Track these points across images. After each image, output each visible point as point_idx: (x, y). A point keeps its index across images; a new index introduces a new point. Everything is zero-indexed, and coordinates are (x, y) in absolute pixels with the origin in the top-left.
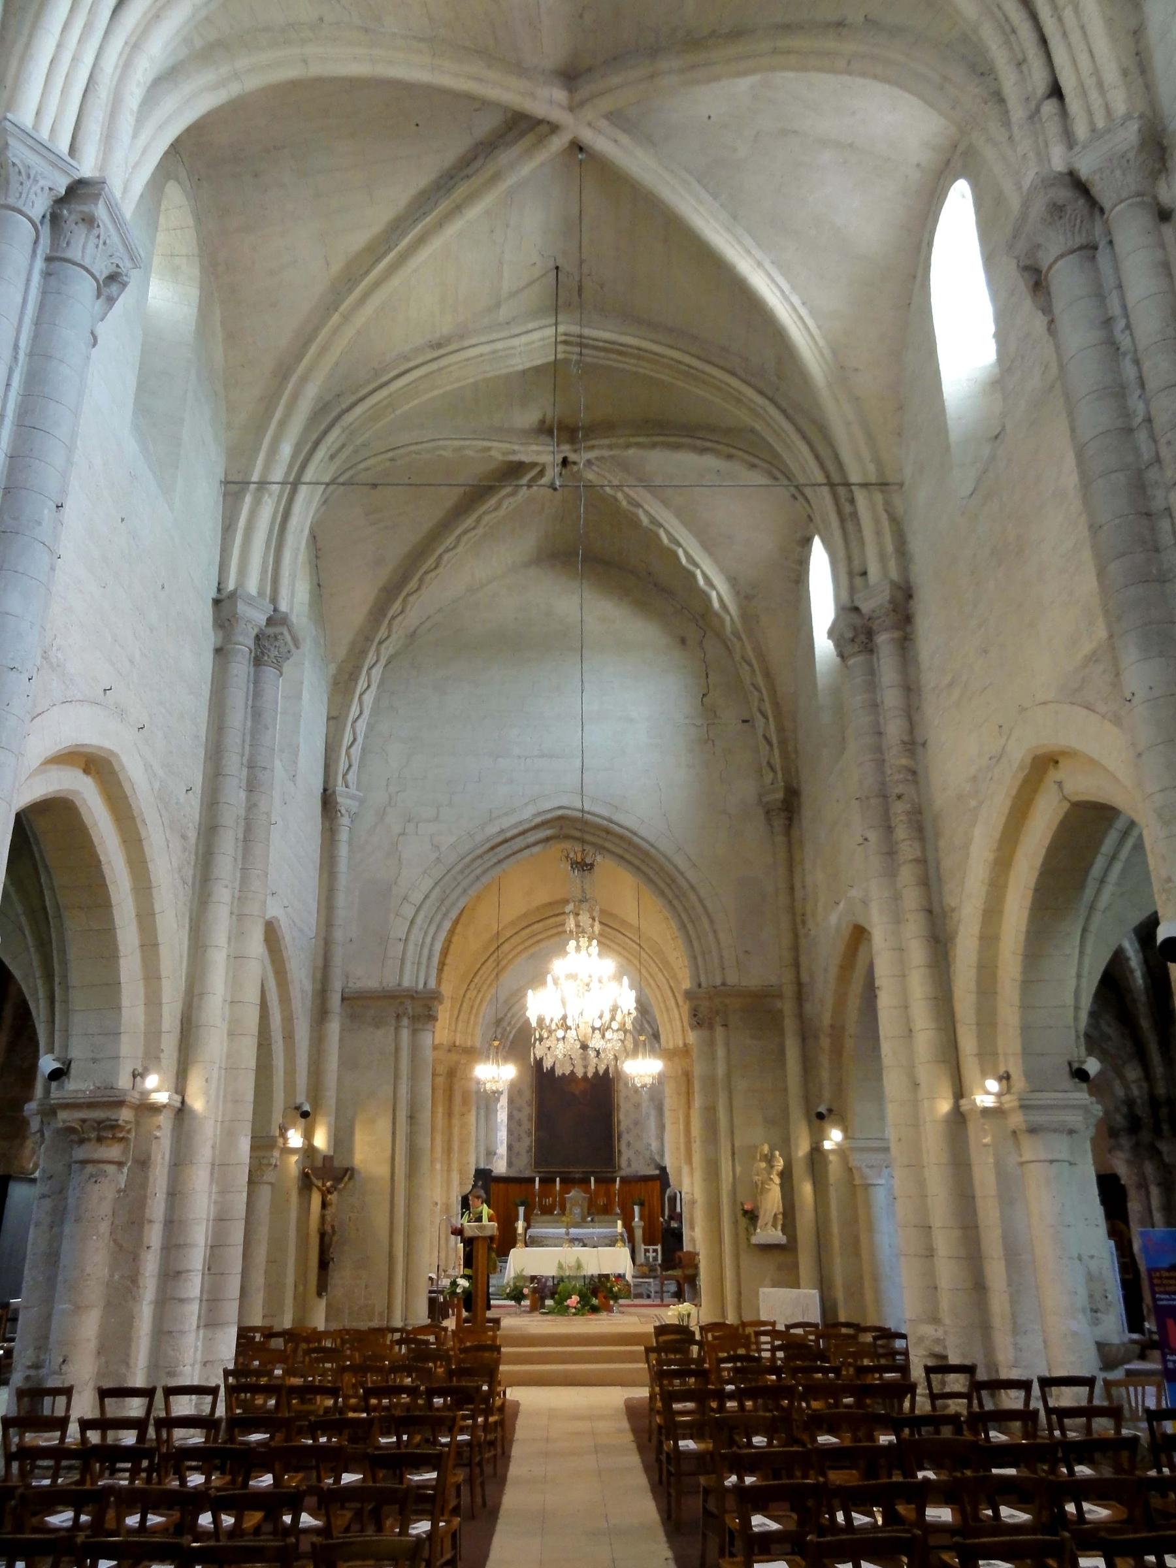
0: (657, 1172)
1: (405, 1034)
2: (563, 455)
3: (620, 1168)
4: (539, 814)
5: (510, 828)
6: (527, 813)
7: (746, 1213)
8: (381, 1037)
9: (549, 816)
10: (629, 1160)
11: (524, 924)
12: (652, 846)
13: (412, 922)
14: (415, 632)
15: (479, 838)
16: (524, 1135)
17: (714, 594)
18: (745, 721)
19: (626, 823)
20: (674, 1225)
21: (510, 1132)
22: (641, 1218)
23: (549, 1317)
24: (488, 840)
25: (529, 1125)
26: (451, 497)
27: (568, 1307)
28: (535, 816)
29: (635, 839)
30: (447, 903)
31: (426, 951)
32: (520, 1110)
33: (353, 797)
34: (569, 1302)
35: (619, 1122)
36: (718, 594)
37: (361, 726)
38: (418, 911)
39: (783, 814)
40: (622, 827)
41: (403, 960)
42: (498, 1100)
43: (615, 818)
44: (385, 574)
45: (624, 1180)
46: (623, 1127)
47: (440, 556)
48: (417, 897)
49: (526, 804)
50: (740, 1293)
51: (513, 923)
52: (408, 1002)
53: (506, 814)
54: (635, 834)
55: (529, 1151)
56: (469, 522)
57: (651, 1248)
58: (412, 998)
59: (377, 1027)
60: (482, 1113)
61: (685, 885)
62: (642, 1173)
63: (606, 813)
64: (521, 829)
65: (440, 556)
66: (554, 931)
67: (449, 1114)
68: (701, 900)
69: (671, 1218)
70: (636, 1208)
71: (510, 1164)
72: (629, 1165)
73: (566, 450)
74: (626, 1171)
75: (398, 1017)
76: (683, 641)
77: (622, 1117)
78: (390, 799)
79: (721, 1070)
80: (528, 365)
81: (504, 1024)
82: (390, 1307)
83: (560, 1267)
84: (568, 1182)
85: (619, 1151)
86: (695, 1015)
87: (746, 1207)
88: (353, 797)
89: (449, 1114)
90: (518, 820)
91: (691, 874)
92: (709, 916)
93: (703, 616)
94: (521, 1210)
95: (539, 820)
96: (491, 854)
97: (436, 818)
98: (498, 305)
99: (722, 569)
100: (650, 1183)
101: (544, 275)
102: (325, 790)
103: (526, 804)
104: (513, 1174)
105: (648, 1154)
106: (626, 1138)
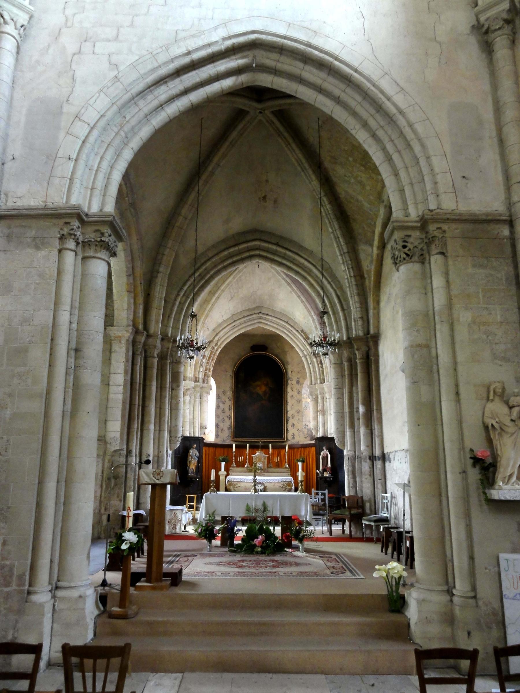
0: (313, 442)
1: (69, 258)
3: (287, 440)
4: (230, 38)
5: (197, 50)
6: (216, 37)
7: (476, 461)
8: (45, 259)
9: (241, 40)
10: (293, 435)
11: (223, 247)
12: (356, 71)
13: (84, 142)
15: (163, 58)
16: (227, 419)
19: (327, 47)
20: (326, 475)
21: (217, 416)
22: (303, 470)
23: (237, 558)
24: (172, 60)
25: (230, 413)
27: (255, 546)
28: (224, 39)
29: (336, 63)
30: (126, 129)
31: (101, 177)
32: (224, 403)
34: (256, 541)
35: (287, 412)
38: (92, 128)
39: (507, 29)
41: (71, 180)
42: (208, 393)
43: (315, 42)
45: (290, 447)
46: (290, 415)
48: (91, 116)
49: (216, 28)
50: (472, 558)
51: (214, 246)
52: (76, 223)
53: (193, 36)
54: (336, 59)
55: (229, 428)
57: (320, 492)
58: (82, 222)
59: (37, 248)
60: (198, 400)
61: (393, 110)
62: (301, 443)
63: (303, 37)
64: (210, 50)
66: (247, 254)
67: (161, 388)
68: (411, 126)
69: (324, 470)
70: (300, 464)
71: (217, 436)
72: (293, 438)
74: (291, 441)
75: (62, 238)
77: (289, 408)
78: (67, 20)
79: (439, 300)
81: (213, 344)
82: (33, 568)
83: (248, 510)
84: (254, 447)
85: (287, 429)
86: (404, 247)
87: (479, 455)
89: (161, 388)
90: (206, 42)
91: (399, 99)
92: (419, 139)
94: (223, 464)
95: (229, 43)
96: (177, 80)
97: (116, 38)
100: (307, 450)
103: (216, 28)
104: (219, 442)
105: (306, 431)
106: (291, 422)
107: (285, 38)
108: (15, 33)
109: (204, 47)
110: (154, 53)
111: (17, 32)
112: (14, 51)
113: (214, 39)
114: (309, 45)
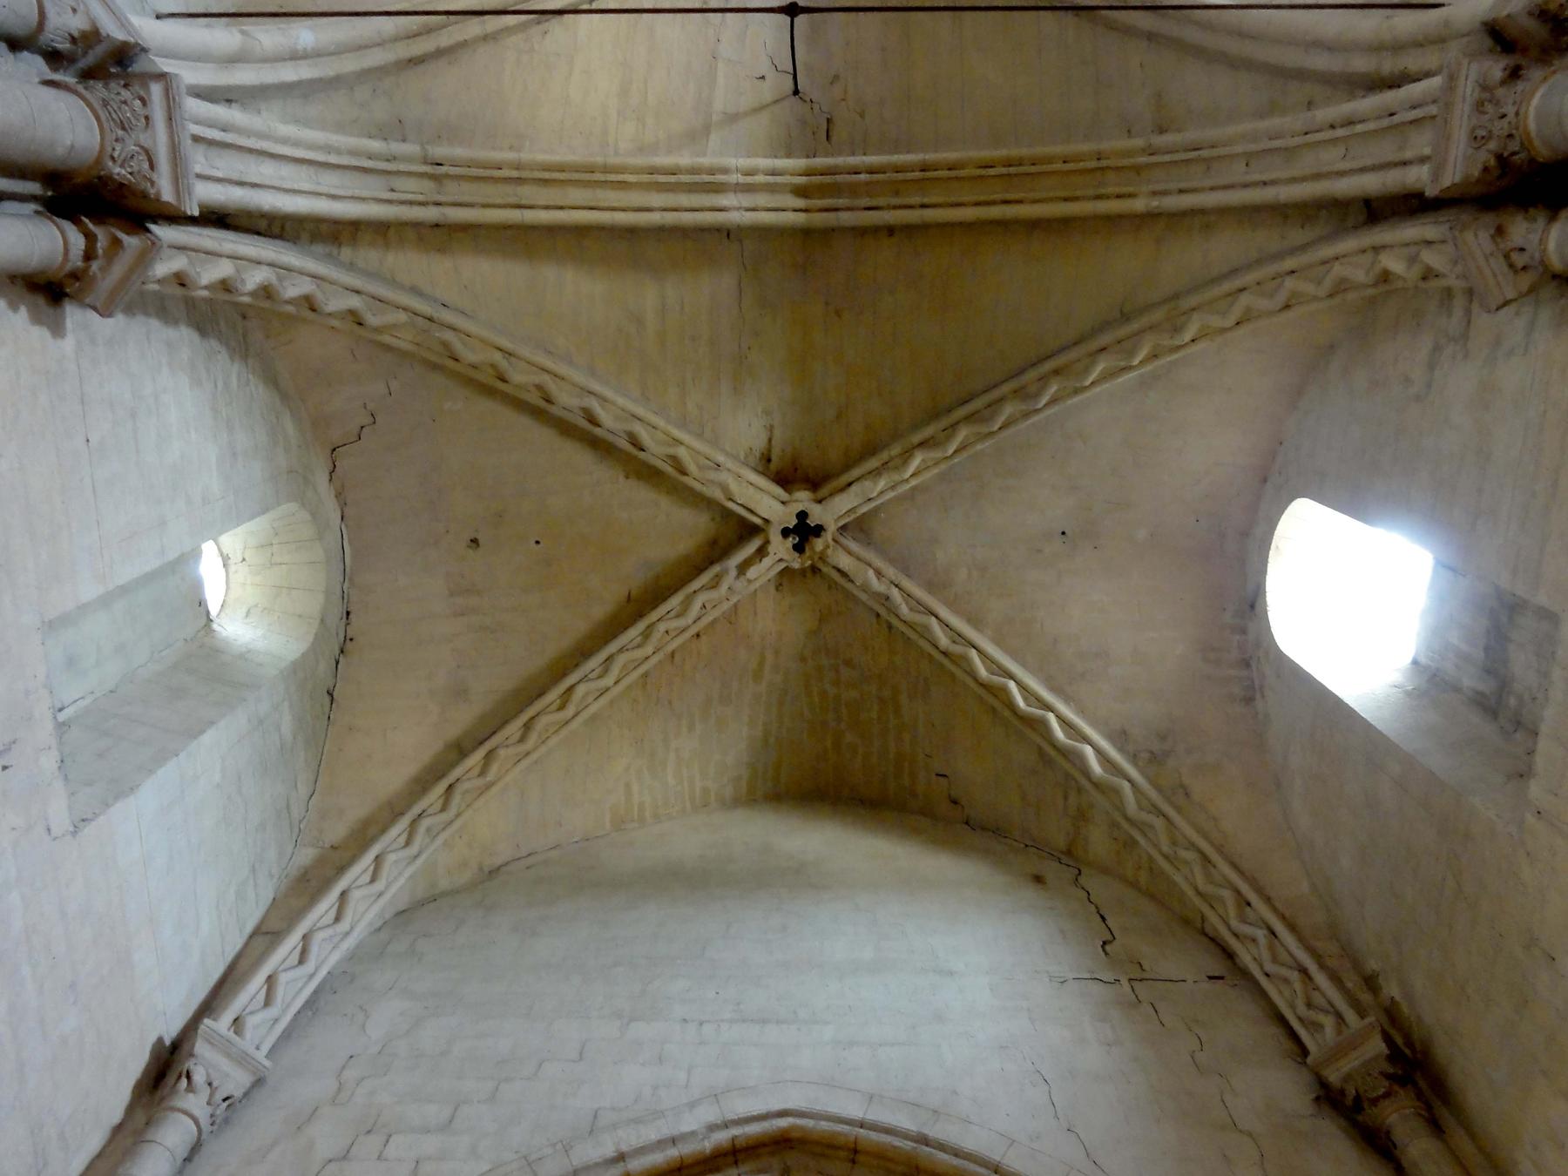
2: (800, 507)
4: (726, 1125)
6: (691, 1122)
9: (754, 1129)
14: (498, 868)
17: (1088, 751)
18: (1210, 978)
19: (969, 1143)
26: (605, 599)
28: (712, 1128)
33: (243, 1059)
36: (1098, 751)
37: (328, 955)
40: (957, 1153)
43: (936, 1131)
44: (462, 718)
47: (571, 689)
49: (692, 1105)
53: (637, 1121)
56: (634, 633)
65: (571, 689)
73: (803, 499)
76: (1038, 879)
78: (339, 1090)
80: (748, 218)
88: (243, 1059)
93: (1069, 853)
95: (722, 1137)
97: (447, 1126)
98: (707, 129)
99: (1094, 723)
101: (776, 102)
102: (176, 1046)
103: (692, 1105)
107: (862, 1125)
108: (202, 1112)
109: (660, 1144)
110: (533, 1157)
111: (209, 1110)
112: (182, 1152)
113: (686, 1128)
114: (924, 1140)
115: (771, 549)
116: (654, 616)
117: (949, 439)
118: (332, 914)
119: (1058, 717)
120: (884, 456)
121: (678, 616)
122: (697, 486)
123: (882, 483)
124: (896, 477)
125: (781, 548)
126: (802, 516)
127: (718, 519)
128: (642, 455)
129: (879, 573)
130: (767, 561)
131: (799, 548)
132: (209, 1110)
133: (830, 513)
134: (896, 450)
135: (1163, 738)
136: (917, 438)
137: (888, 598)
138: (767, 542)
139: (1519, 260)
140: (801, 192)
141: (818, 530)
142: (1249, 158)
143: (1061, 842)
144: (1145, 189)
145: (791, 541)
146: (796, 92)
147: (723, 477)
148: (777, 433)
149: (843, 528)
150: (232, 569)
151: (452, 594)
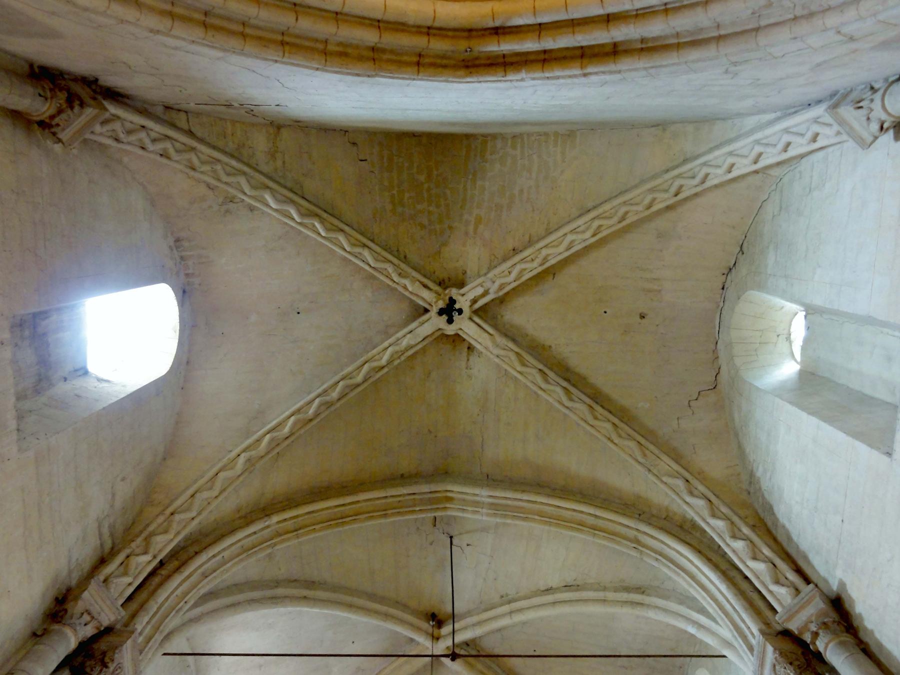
36: (268, 205)
73: (450, 330)
115: (468, 304)
116: (540, 269)
117: (368, 373)
118: (763, 157)
119: (293, 219)
120: (403, 358)
121: (525, 269)
122: (511, 345)
123: (405, 343)
124: (397, 348)
125: (463, 303)
126: (450, 321)
127: (499, 317)
128: (541, 366)
129: (405, 288)
130: (471, 296)
131: (452, 301)
132: (873, 106)
133: (434, 323)
134: (396, 362)
135: (227, 211)
136: (386, 370)
137: (400, 274)
138: (471, 306)
139: (86, 618)
140: (449, 499)
141: (441, 312)
142: (224, 563)
143: (285, 133)
144: (273, 528)
145: (457, 306)
146: (451, 537)
147: (496, 351)
148: (463, 364)
149: (426, 311)
150: (786, 332)
151: (660, 291)
